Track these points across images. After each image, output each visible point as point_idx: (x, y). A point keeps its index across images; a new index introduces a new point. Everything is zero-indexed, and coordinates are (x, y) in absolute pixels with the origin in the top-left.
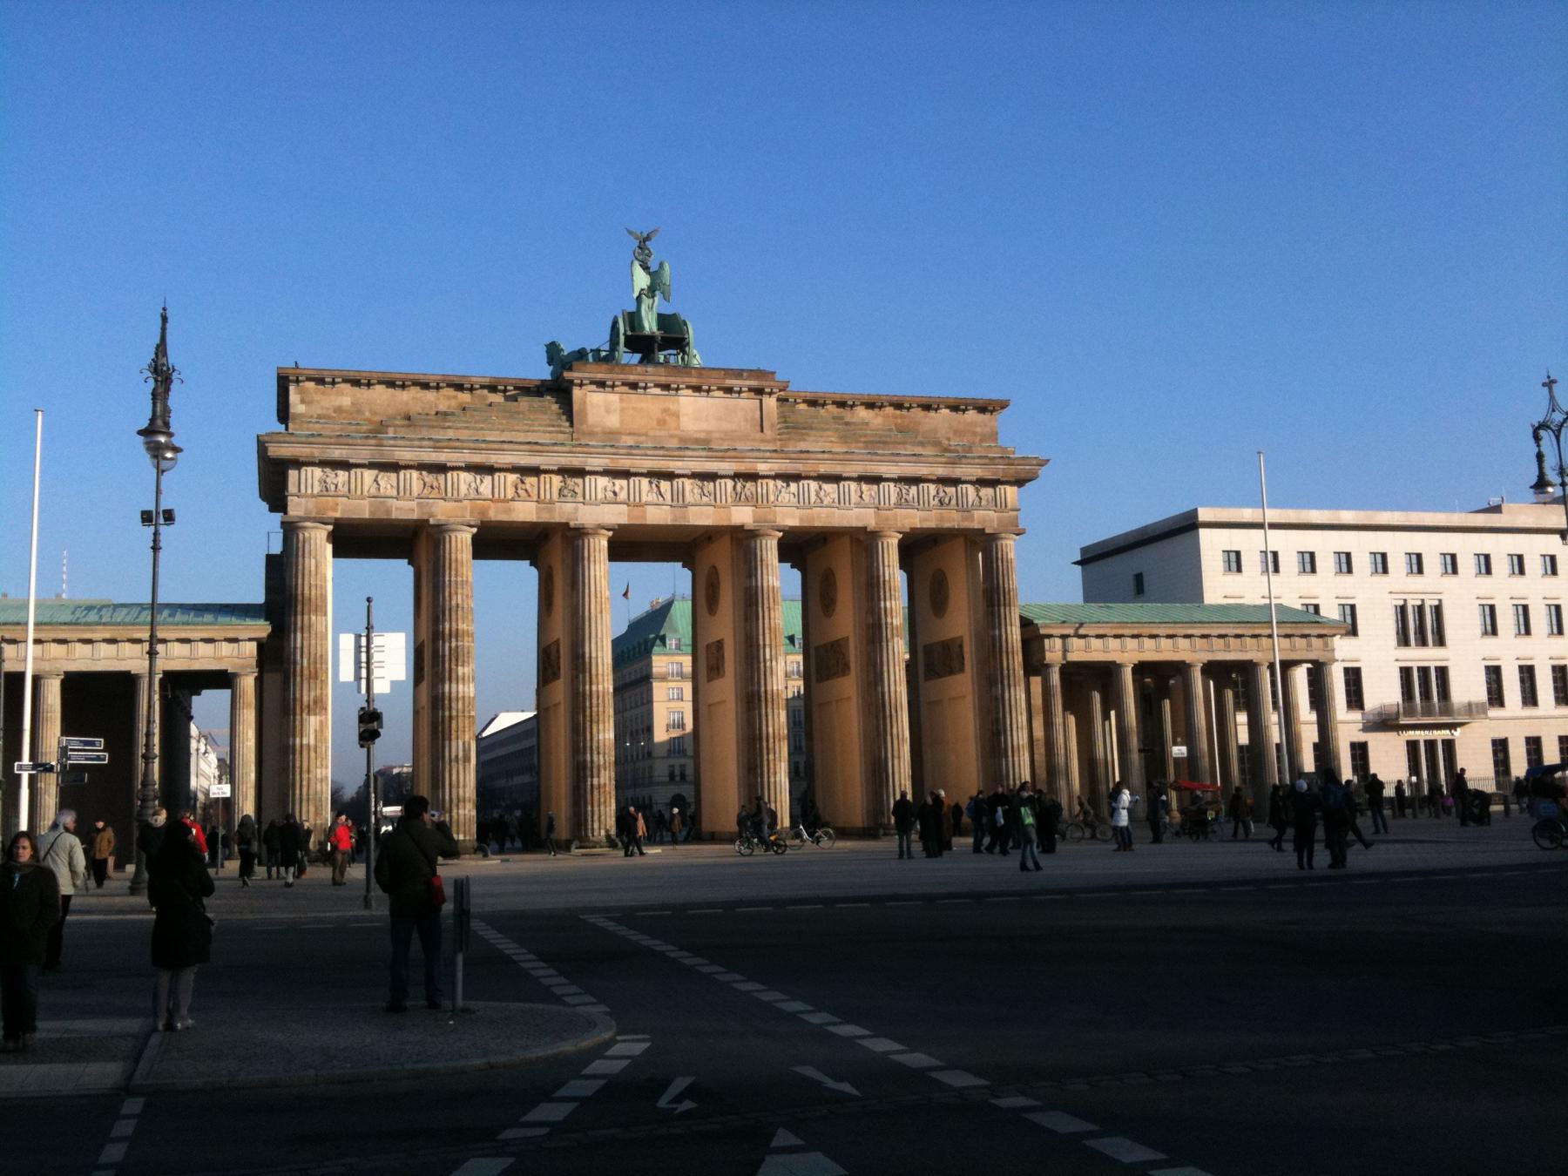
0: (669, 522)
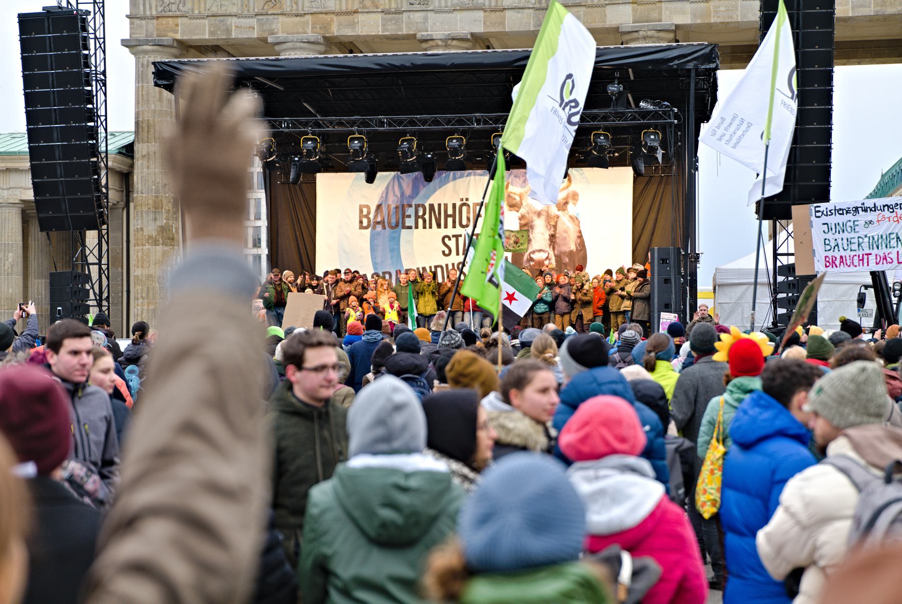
0: (532, 29)
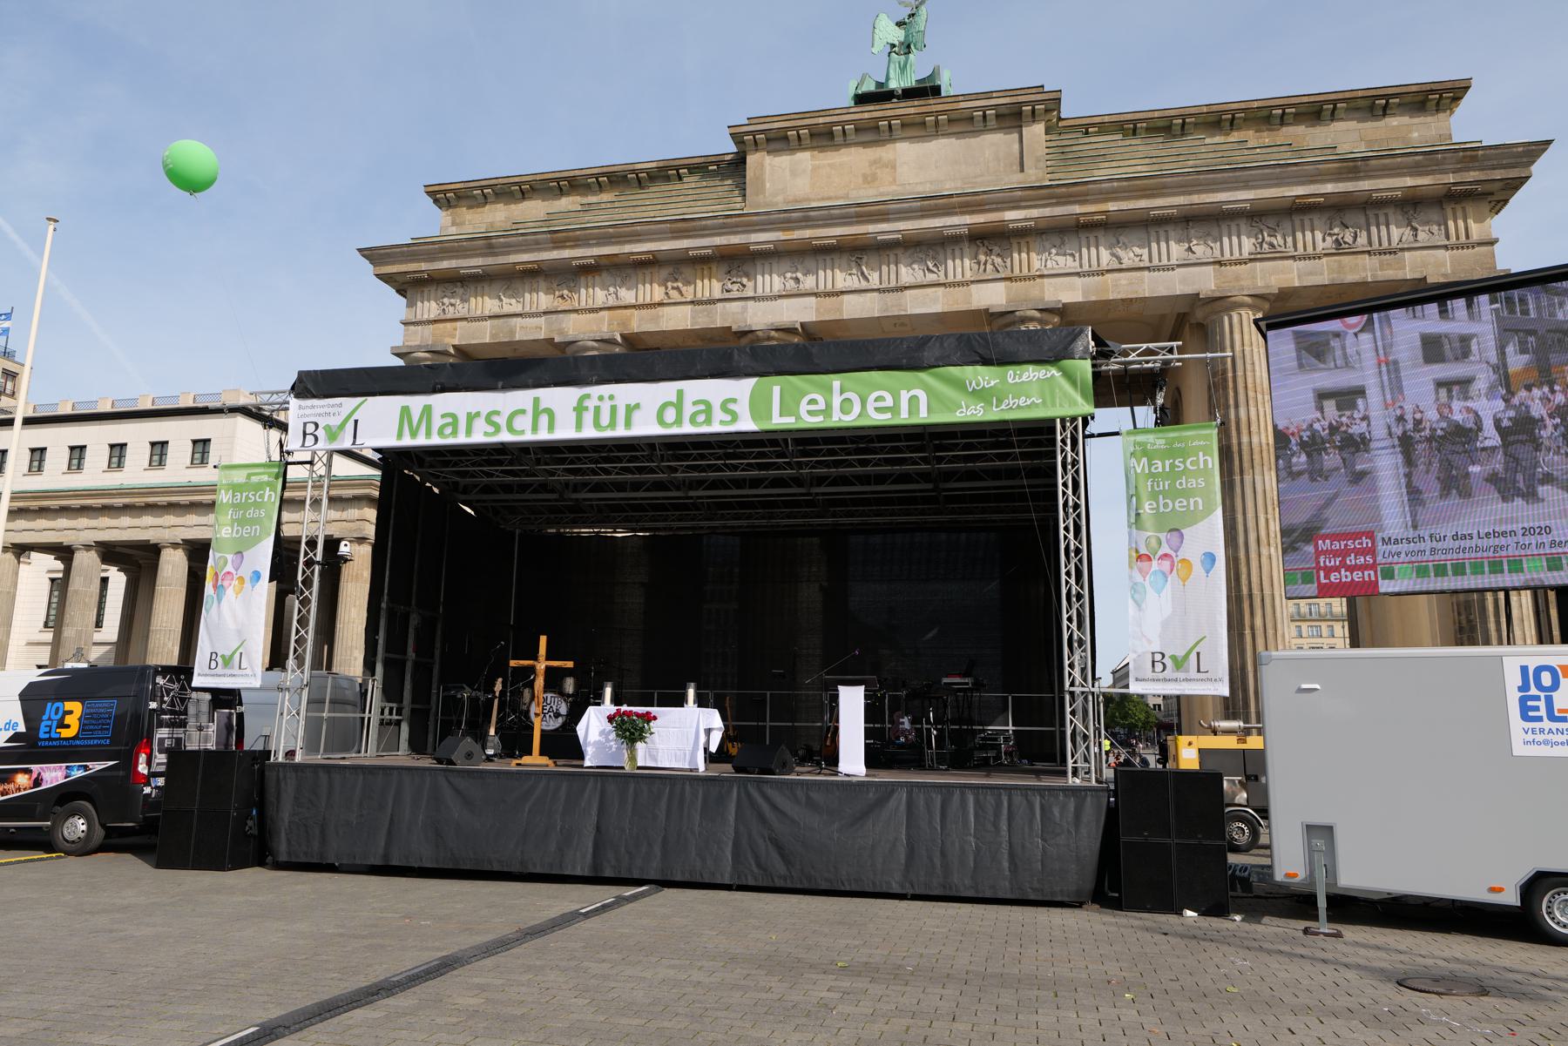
0: (876, 315)
